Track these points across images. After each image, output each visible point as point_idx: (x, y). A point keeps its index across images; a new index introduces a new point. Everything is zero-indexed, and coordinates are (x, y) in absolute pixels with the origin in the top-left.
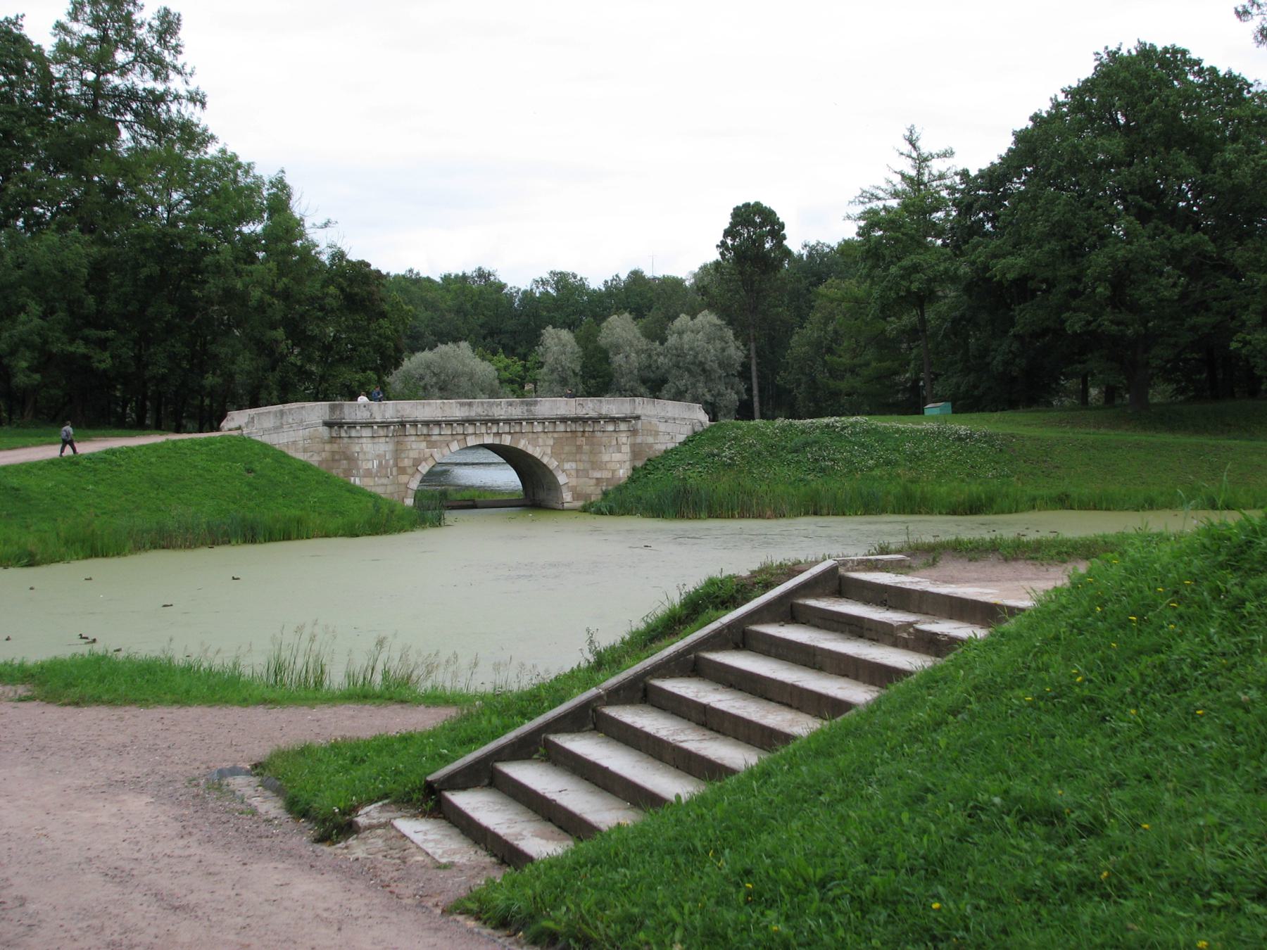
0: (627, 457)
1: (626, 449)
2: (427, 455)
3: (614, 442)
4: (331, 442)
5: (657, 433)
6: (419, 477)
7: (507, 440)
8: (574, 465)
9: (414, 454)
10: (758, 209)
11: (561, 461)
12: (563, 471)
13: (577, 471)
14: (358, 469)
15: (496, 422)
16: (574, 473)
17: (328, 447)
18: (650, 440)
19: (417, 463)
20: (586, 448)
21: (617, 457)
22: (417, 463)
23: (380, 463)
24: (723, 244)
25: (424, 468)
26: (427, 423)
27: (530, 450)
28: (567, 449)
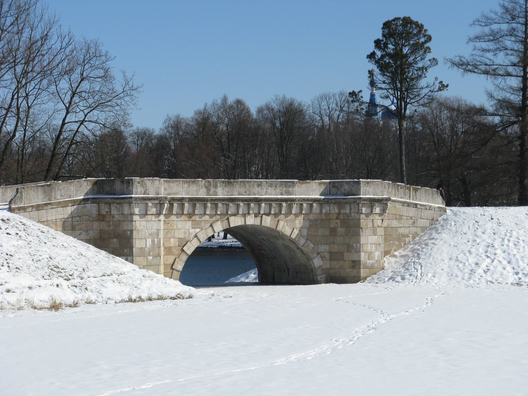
0: (381, 240)
1: (381, 231)
2: (193, 235)
3: (370, 225)
4: (98, 220)
5: (401, 216)
6: (184, 258)
7: (268, 222)
8: (327, 248)
9: (180, 234)
10: (407, 21)
11: (316, 244)
12: (318, 254)
13: (330, 253)
14: (131, 248)
15: (258, 201)
16: (327, 255)
17: (96, 225)
18: (395, 223)
19: (183, 243)
20: (341, 230)
21: (373, 239)
22: (183, 243)
23: (153, 241)
24: (372, 56)
25: (190, 249)
26: (193, 201)
27: (287, 231)
28: (321, 232)
